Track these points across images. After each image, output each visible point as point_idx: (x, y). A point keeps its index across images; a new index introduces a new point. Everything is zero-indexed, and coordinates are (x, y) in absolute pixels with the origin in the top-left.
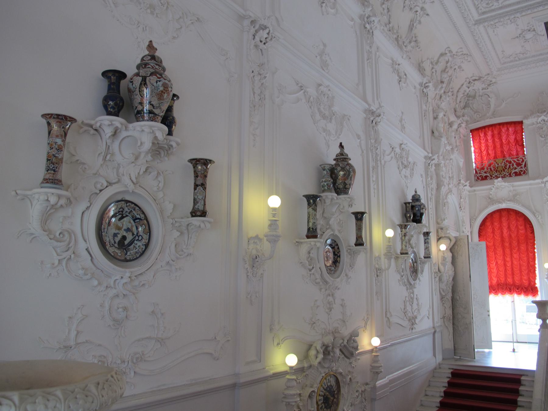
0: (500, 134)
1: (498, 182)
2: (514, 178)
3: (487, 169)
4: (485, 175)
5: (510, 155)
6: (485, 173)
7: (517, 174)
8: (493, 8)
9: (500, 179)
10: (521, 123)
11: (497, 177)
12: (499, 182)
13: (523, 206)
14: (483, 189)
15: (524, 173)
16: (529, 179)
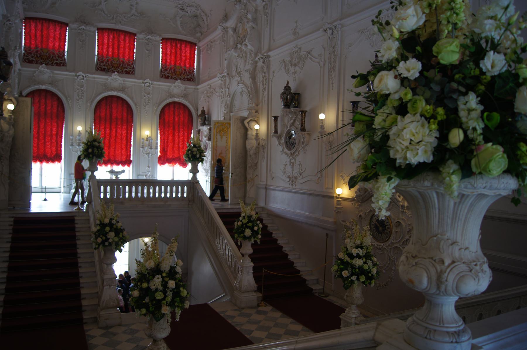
1: (43, 67)
2: (55, 67)
3: (34, 54)
4: (32, 59)
6: (32, 57)
9: (44, 65)
11: (41, 64)
15: (63, 65)
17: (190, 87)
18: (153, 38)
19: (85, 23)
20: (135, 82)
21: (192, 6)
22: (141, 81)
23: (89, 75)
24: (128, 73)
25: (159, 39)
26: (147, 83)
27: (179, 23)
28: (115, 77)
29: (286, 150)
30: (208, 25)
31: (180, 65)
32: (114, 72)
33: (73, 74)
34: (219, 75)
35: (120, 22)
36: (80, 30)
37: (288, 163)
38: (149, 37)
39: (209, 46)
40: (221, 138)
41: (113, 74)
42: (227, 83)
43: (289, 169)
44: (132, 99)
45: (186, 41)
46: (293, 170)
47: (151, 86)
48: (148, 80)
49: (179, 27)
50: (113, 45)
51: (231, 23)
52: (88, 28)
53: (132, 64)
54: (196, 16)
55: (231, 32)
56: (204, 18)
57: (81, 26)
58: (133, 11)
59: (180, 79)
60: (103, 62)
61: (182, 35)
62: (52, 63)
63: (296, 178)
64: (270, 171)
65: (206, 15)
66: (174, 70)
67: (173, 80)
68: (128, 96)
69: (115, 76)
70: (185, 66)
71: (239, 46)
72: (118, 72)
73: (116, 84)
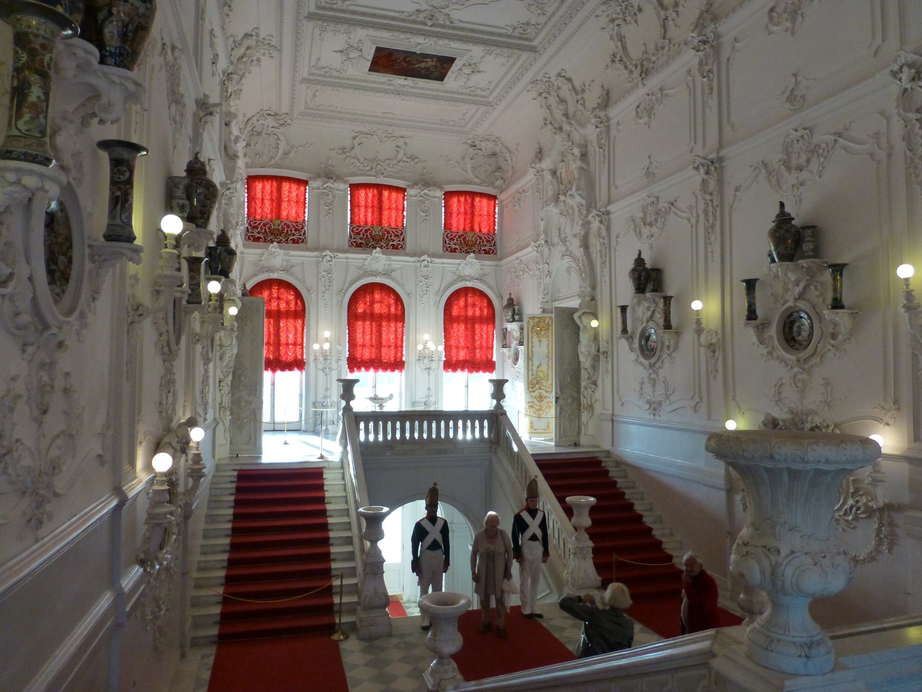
8: (335, 6)
18: (431, 193)
21: (487, 140)
24: (395, 247)
28: (377, 255)
29: (641, 359)
30: (513, 167)
32: (375, 248)
34: (533, 244)
37: (646, 380)
38: (426, 191)
39: (516, 199)
40: (540, 341)
42: (546, 256)
43: (648, 388)
46: (654, 391)
51: (547, 164)
52: (336, 185)
53: (402, 234)
54: (494, 154)
55: (548, 177)
56: (507, 155)
57: (327, 182)
58: (400, 156)
59: (474, 252)
63: (660, 403)
64: (618, 392)
65: (510, 152)
66: (464, 239)
67: (463, 254)
68: (397, 282)
71: (562, 198)
72: (381, 247)
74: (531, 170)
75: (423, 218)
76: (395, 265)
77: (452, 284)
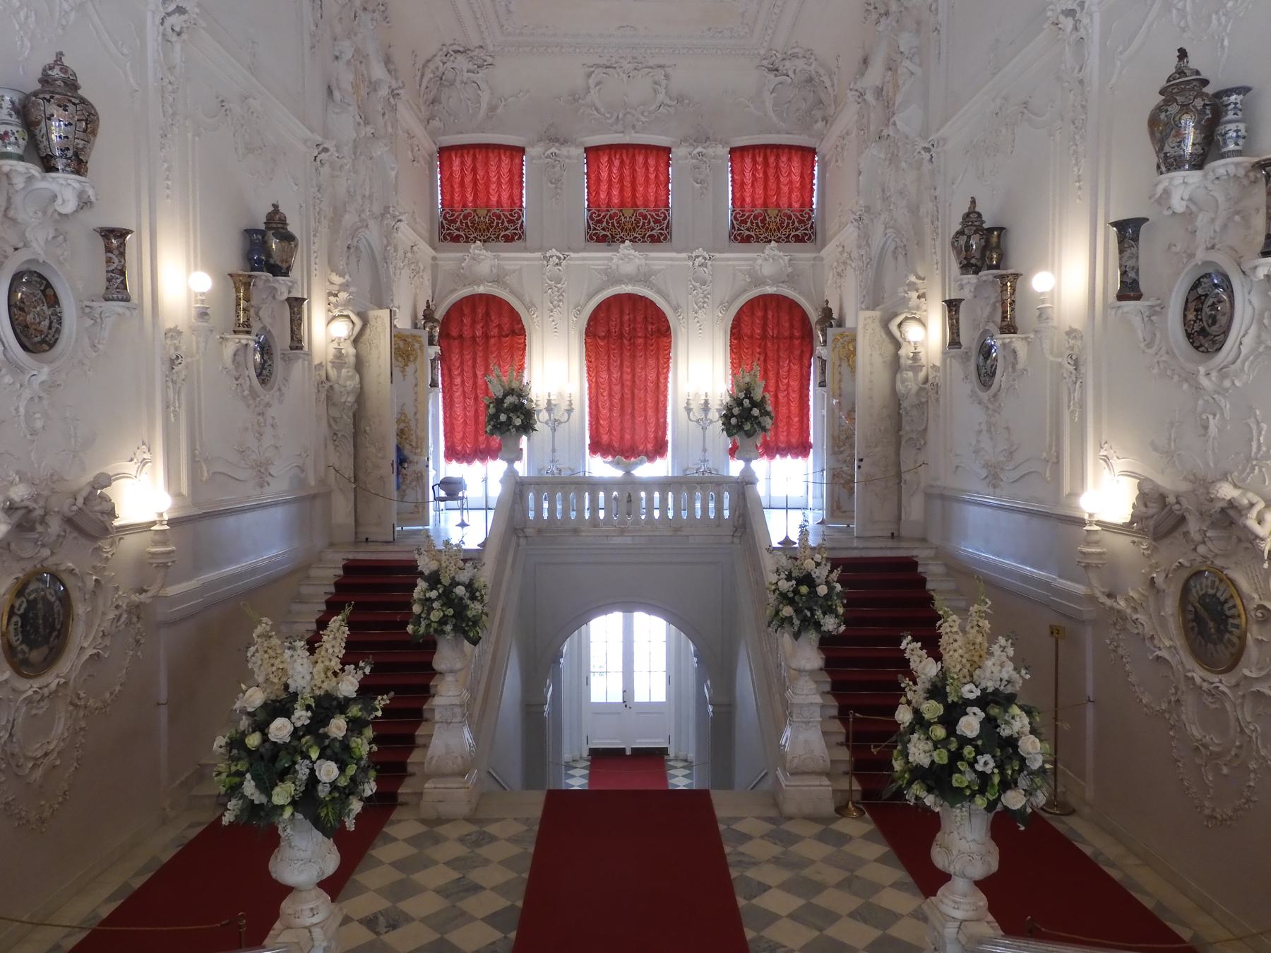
0: (486, 164)
2: (502, 244)
5: (499, 204)
6: (458, 229)
7: (508, 239)
10: (522, 151)
12: (476, 248)
13: (512, 292)
14: (451, 257)
15: (519, 238)
16: (526, 250)
17: (802, 255)
18: (710, 151)
19: (557, 140)
20: (672, 259)
21: (794, 56)
22: (684, 255)
23: (572, 255)
24: (655, 240)
25: (724, 152)
26: (697, 257)
27: (769, 105)
28: (626, 252)
31: (778, 205)
33: (538, 255)
35: (634, 127)
36: (548, 157)
41: (622, 246)
44: (666, 297)
45: (790, 147)
47: (709, 263)
48: (700, 251)
49: (772, 114)
50: (621, 179)
53: (665, 218)
60: (600, 222)
61: (778, 132)
62: (497, 238)
66: (763, 221)
68: (659, 292)
69: (626, 248)
70: (790, 205)
73: (628, 268)
74: (850, 94)
75: (702, 190)
76: (657, 265)
77: (745, 291)
